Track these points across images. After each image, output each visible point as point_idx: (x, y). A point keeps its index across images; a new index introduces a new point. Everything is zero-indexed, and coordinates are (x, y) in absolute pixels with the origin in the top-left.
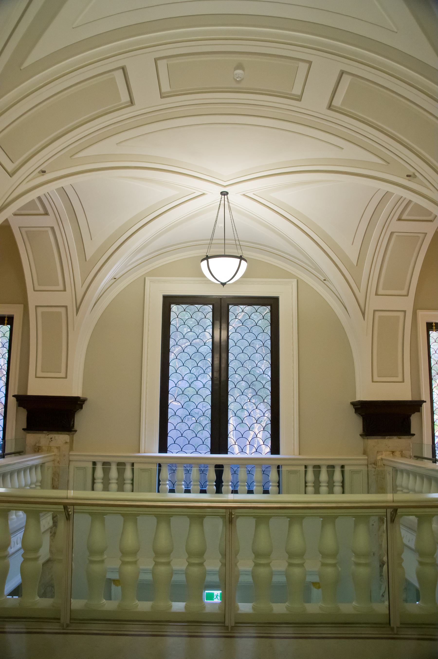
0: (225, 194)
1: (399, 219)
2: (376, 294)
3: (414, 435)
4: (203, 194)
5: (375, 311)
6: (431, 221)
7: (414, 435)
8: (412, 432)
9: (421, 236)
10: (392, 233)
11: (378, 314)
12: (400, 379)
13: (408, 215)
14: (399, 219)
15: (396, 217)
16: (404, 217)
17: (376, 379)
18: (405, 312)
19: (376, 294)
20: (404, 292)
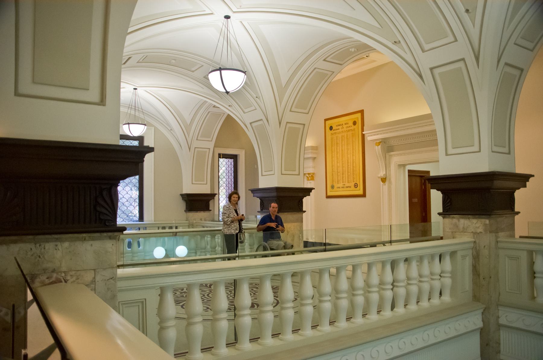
0: (227, 17)
1: (324, 60)
2: (290, 111)
3: (305, 211)
4: (212, 14)
5: (287, 122)
6: (341, 65)
7: (305, 211)
8: (304, 210)
9: (330, 73)
10: (315, 68)
11: (289, 125)
12: (297, 173)
13: (332, 58)
14: (324, 60)
15: (323, 59)
16: (327, 60)
17: (284, 172)
18: (304, 125)
19: (290, 111)
20: (306, 111)
